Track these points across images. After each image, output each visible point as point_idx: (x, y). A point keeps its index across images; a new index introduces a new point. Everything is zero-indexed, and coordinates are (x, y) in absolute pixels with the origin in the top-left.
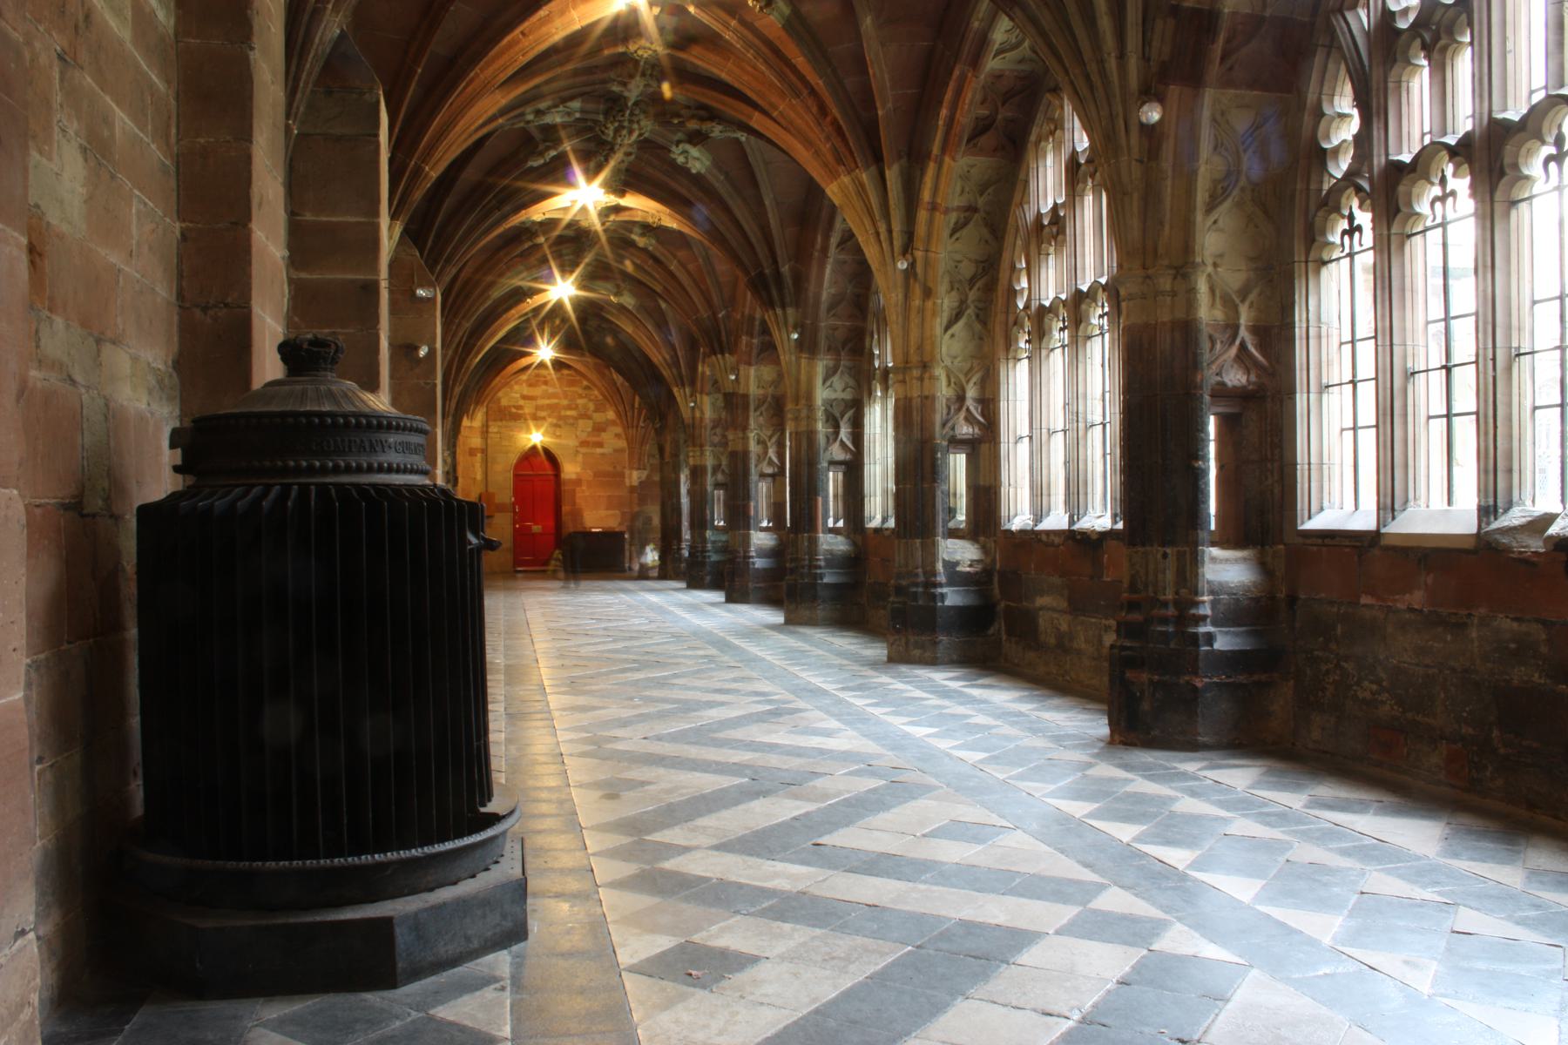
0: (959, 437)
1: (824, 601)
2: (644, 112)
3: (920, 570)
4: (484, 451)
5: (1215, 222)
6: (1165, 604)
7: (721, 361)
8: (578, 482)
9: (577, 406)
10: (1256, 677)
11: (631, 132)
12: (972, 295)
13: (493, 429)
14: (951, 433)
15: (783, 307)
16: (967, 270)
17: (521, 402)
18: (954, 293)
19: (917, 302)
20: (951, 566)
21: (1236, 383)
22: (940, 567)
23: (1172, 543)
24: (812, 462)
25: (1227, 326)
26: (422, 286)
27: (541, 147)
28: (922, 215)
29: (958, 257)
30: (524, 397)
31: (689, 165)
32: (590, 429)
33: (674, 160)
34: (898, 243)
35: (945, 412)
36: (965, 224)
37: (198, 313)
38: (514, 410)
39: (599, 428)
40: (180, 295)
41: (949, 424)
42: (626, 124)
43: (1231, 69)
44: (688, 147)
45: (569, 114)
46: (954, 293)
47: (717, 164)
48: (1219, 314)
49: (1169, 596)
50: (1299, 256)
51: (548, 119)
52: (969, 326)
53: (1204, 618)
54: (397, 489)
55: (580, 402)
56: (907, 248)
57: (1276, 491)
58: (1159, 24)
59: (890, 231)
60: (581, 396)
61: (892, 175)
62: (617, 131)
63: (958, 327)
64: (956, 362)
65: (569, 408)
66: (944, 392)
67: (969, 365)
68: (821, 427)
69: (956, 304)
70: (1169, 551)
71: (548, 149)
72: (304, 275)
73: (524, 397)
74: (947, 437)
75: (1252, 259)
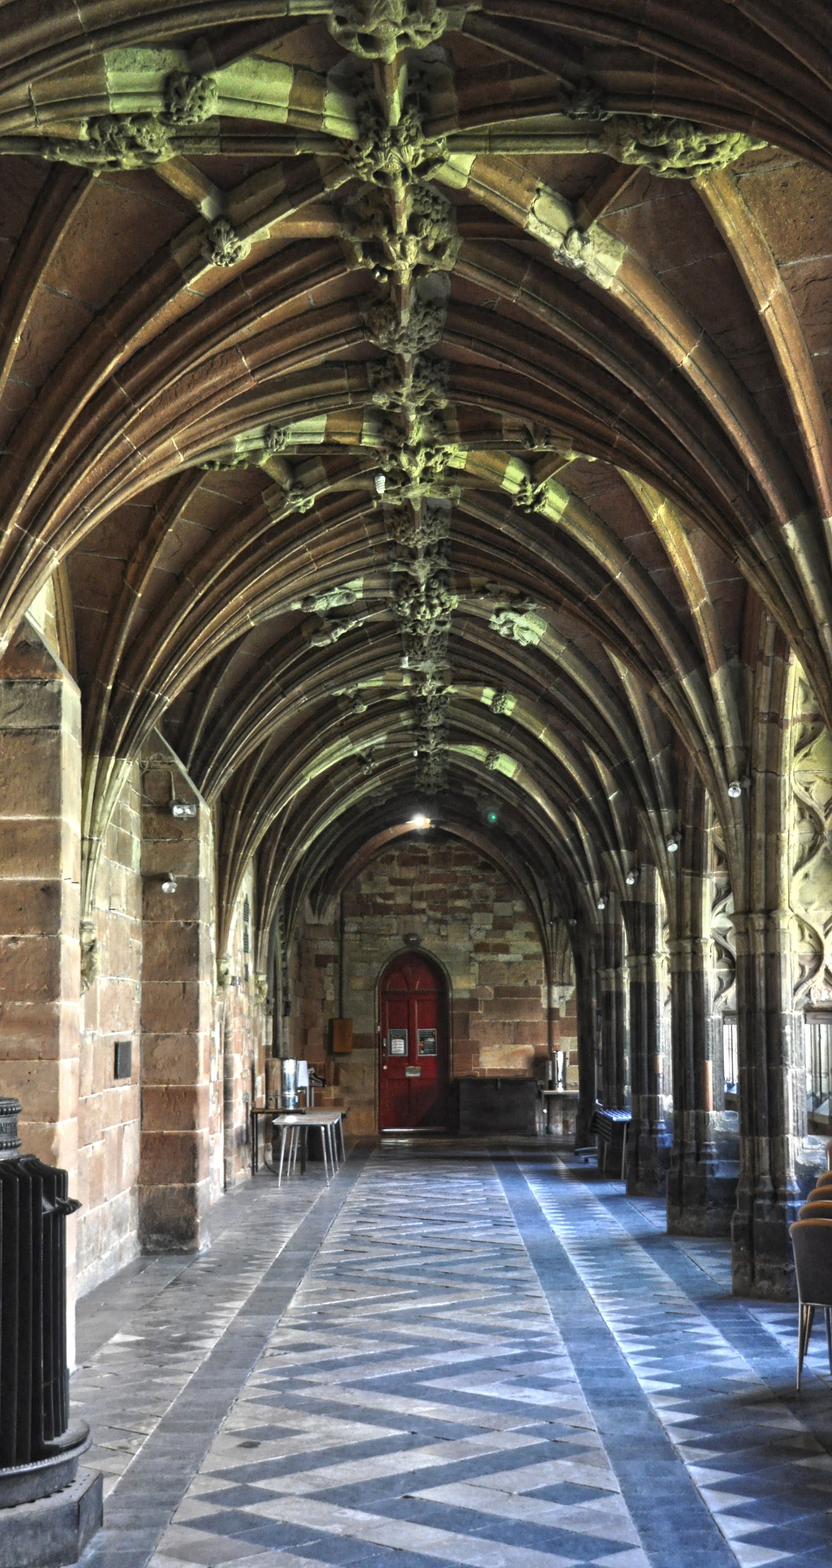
0: (816, 1005)
1: (716, 1204)
2: (446, 584)
3: (767, 1177)
4: (338, 959)
7: (615, 858)
8: (472, 1003)
9: (470, 893)
11: (432, 608)
13: (351, 927)
14: (806, 1000)
15: (657, 809)
17: (390, 889)
19: (760, 835)
22: (792, 1173)
24: (700, 1014)
26: (180, 803)
27: (327, 624)
28: (762, 728)
29: (809, 777)
30: (394, 882)
31: (516, 637)
32: (489, 927)
33: (496, 632)
34: (732, 761)
35: (797, 972)
36: (814, 737)
38: (380, 900)
39: (502, 925)
42: (423, 600)
44: (511, 616)
45: (348, 596)
46: (805, 824)
47: (556, 631)
55: (475, 887)
56: (746, 771)
59: (721, 748)
60: (476, 879)
62: (415, 607)
63: (810, 867)
65: (458, 895)
71: (335, 626)
73: (394, 882)
74: (801, 1006)
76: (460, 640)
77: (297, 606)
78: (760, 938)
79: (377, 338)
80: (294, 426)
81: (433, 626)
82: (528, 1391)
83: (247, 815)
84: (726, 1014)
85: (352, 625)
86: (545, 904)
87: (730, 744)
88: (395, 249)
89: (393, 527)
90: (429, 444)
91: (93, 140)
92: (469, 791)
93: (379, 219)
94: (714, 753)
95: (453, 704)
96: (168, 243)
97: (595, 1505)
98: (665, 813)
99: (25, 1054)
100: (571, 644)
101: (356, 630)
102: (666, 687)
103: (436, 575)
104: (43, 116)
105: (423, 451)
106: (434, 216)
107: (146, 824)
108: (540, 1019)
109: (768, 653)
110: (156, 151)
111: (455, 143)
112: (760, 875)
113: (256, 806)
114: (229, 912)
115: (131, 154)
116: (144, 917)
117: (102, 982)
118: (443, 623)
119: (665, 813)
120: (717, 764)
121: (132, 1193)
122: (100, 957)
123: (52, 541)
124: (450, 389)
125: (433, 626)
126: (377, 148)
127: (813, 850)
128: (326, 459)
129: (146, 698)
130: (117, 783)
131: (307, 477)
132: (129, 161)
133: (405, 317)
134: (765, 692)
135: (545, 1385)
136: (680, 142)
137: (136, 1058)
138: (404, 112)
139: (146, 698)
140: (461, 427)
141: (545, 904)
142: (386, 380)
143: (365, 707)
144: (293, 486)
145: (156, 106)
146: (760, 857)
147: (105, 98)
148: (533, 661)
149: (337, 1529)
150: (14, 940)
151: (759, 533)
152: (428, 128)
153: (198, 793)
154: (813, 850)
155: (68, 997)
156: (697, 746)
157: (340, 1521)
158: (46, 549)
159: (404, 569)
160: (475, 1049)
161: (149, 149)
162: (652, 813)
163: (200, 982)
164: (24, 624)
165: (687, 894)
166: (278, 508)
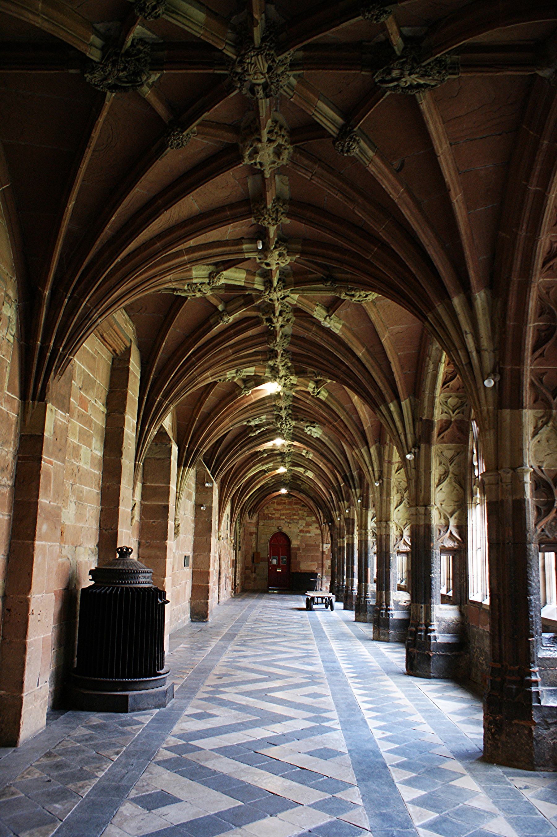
0: (401, 551)
2: (291, 418)
3: (384, 604)
4: (257, 534)
5: (441, 489)
8: (298, 549)
9: (299, 514)
10: (454, 653)
11: (287, 425)
12: (406, 495)
13: (261, 524)
15: (355, 489)
16: (404, 484)
17: (274, 512)
18: (399, 494)
19: (385, 498)
20: (397, 603)
21: (450, 546)
22: (391, 602)
23: (425, 603)
24: (366, 554)
25: (446, 525)
26: (207, 482)
27: (254, 429)
28: (386, 465)
29: (400, 480)
30: (275, 510)
31: (312, 435)
32: (304, 525)
34: (376, 475)
35: (395, 540)
37: (104, 531)
38: (270, 515)
39: (308, 524)
40: (100, 526)
41: (397, 546)
43: (443, 437)
44: (311, 428)
45: (261, 421)
46: (399, 494)
47: (325, 433)
48: (443, 521)
49: (423, 622)
50: (469, 501)
52: (405, 506)
53: (434, 630)
54: (141, 589)
55: (300, 512)
56: (381, 477)
57: (465, 585)
58: (417, 424)
59: (373, 470)
60: (300, 510)
61: (373, 450)
62: (281, 425)
64: (400, 521)
66: (395, 533)
67: (405, 522)
69: (399, 498)
70: (423, 606)
71: (257, 430)
72: (146, 503)
73: (275, 510)
75: (456, 502)
76: (296, 435)
77: (245, 423)
80: (245, 370)
81: (287, 431)
82: (306, 666)
83: (229, 487)
84: (375, 553)
85: (262, 429)
86: (322, 518)
87: (376, 469)
88: (275, 320)
90: (286, 376)
91: (188, 289)
92: (299, 482)
93: (271, 311)
94: (371, 472)
95: (293, 455)
96: (209, 317)
97: (323, 699)
98: (358, 490)
99: (157, 557)
100: (329, 438)
101: (263, 431)
102: (357, 451)
103: (288, 415)
104: (174, 284)
105: (283, 378)
106: (287, 311)
107: (197, 488)
108: (319, 554)
109: (388, 442)
110: (206, 292)
112: (384, 509)
113: (231, 485)
114: (222, 517)
115: (199, 293)
116: (195, 517)
117: (181, 536)
118: (290, 430)
119: (358, 490)
120: (372, 475)
121: (189, 602)
122: (181, 529)
123: (171, 402)
124: (292, 360)
125: (287, 431)
126: (270, 292)
128: (255, 380)
129: (198, 450)
130: (188, 475)
131: (248, 385)
132: (198, 295)
133: (278, 339)
135: (312, 664)
136: (358, 293)
137: (191, 560)
138: (278, 283)
139: (198, 450)
140: (296, 371)
141: (322, 518)
142: (273, 357)
143: (266, 455)
144: (245, 387)
145: (207, 281)
146: (384, 504)
147: (192, 279)
148: (317, 442)
149: (244, 703)
150: (154, 522)
151: (382, 406)
152: (285, 287)
153: (213, 480)
154: (401, 503)
155: (170, 540)
156: (366, 470)
157: (245, 701)
158: (169, 405)
159: (278, 413)
160: (299, 563)
161: (204, 292)
162: (353, 490)
163: (212, 538)
164: (162, 426)
165: (364, 515)
166: (240, 394)
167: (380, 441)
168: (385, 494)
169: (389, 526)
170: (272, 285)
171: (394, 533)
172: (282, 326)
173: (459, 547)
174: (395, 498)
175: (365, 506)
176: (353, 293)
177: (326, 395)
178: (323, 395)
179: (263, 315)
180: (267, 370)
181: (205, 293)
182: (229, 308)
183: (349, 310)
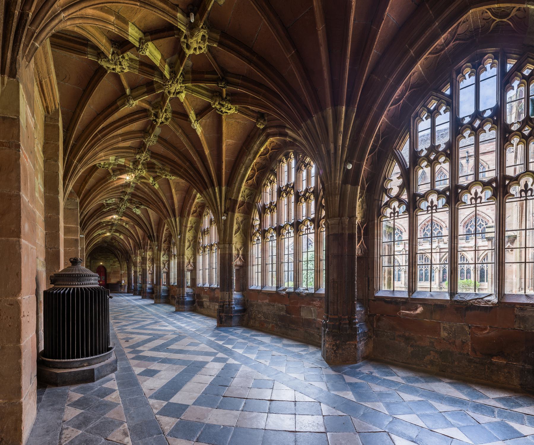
6: (227, 302)
8: (110, 273)
11: (125, 205)
13: (92, 262)
15: (155, 242)
19: (182, 244)
24: (160, 272)
27: (106, 207)
34: (178, 232)
51: (108, 202)
52: (191, 249)
56: (180, 234)
59: (177, 230)
61: (177, 219)
62: (122, 205)
63: (188, 249)
68: (162, 266)
78: (181, 259)
79: (145, 140)
89: (125, 188)
90: (141, 169)
91: (112, 60)
94: (176, 231)
98: (156, 242)
102: (169, 220)
108: (120, 275)
110: (125, 68)
111: (186, 89)
112: (182, 250)
115: (119, 67)
119: (156, 242)
124: (151, 157)
127: (189, 247)
131: (115, 173)
134: (185, 222)
152: (184, 82)
154: (189, 247)
167: (182, 215)
168: (182, 242)
169: (184, 258)
170: (176, 77)
171: (186, 261)
172: (162, 123)
173: (243, 265)
174: (187, 244)
175: (159, 250)
176: (224, 103)
177: (158, 186)
178: (157, 186)
179: (153, 110)
180: (131, 163)
181: (123, 69)
182: (134, 94)
183: (208, 120)
